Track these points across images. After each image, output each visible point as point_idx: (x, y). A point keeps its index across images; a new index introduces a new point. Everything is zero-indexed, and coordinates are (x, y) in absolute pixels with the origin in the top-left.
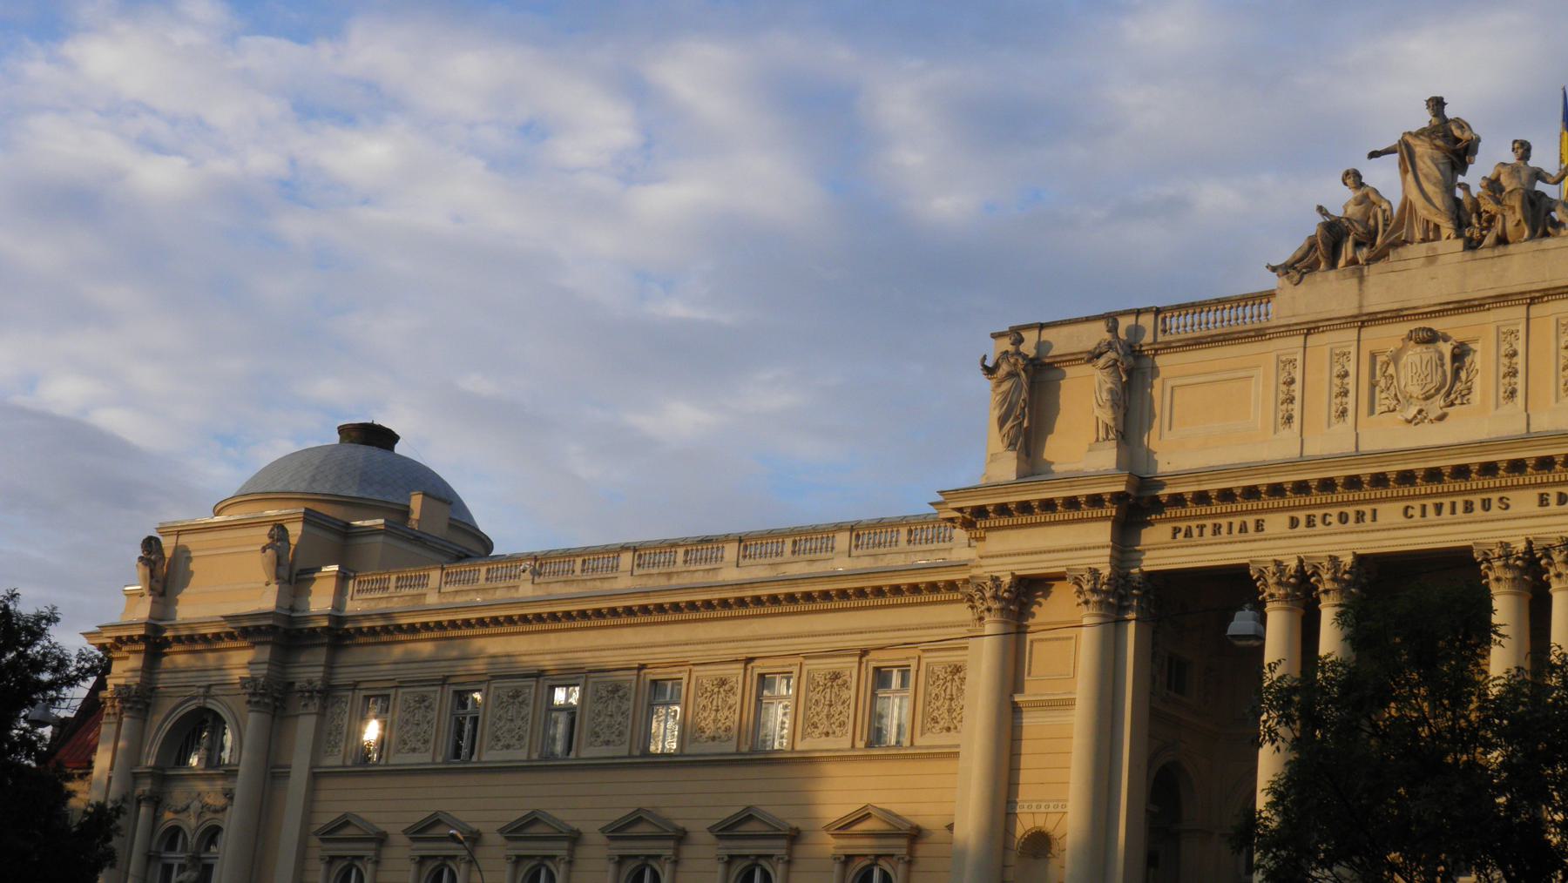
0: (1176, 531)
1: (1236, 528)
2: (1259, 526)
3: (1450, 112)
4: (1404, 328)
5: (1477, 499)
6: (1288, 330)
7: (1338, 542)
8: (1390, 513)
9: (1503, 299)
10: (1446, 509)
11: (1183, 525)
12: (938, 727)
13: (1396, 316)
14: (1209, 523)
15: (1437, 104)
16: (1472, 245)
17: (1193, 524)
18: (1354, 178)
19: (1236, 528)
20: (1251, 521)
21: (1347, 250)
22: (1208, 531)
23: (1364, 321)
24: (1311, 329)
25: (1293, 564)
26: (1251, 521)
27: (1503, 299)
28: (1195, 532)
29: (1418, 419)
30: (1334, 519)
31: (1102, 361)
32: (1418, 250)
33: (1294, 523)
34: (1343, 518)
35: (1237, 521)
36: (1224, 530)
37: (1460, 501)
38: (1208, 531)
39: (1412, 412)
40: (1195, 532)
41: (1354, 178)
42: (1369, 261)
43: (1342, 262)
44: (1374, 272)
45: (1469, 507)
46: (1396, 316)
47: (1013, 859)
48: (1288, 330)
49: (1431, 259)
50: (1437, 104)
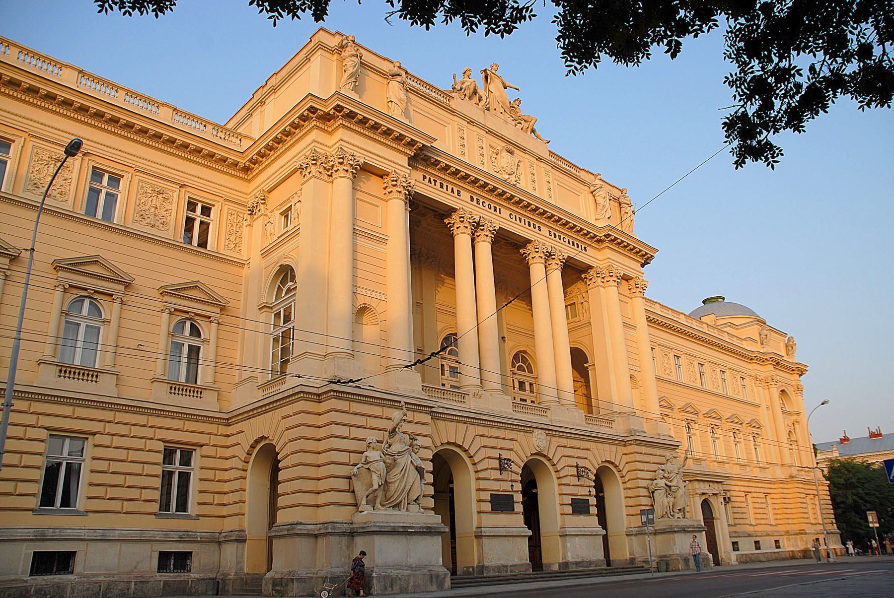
12: (144, 222)
23: (489, 132)
27: (531, 154)
28: (433, 182)
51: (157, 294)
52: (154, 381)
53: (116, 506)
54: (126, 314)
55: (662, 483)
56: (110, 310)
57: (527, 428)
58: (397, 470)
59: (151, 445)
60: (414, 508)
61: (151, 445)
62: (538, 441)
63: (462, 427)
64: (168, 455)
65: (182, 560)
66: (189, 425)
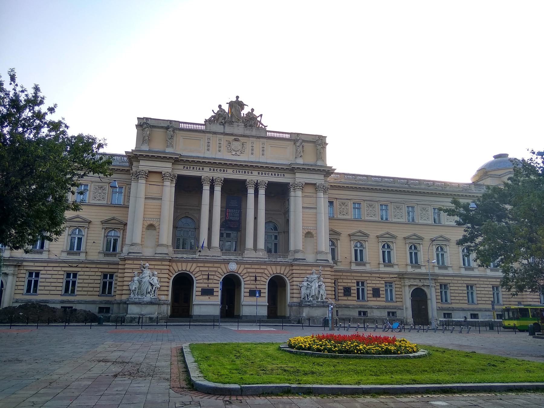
0: (184, 167)
1: (198, 169)
2: (203, 169)
3: (239, 100)
4: (234, 138)
5: (247, 171)
6: (209, 132)
7: (220, 175)
8: (230, 171)
9: (253, 137)
10: (241, 172)
11: (186, 166)
13: (232, 135)
14: (192, 167)
15: (237, 97)
16: (246, 126)
17: (188, 166)
18: (220, 106)
19: (198, 169)
20: (201, 168)
21: (221, 120)
22: (192, 168)
24: (215, 133)
25: (211, 178)
26: (201, 168)
27: (253, 137)
28: (189, 168)
29: (236, 154)
30: (219, 170)
31: (170, 129)
32: (235, 124)
33: (210, 170)
34: (220, 170)
35: (198, 167)
36: (195, 169)
37: (243, 171)
38: (192, 168)
39: (234, 153)
40: (189, 168)
41: (220, 106)
42: (225, 123)
43: (220, 121)
44: (226, 125)
45: (245, 173)
46: (232, 135)
47: (144, 230)
48: (209, 132)
49: (238, 126)
50: (237, 97)
51: (100, 223)
52: (99, 253)
53: (85, 293)
54: (89, 232)
55: (305, 284)
56: (84, 232)
57: (227, 262)
58: (142, 283)
59: (97, 274)
60: (148, 295)
61: (97, 274)
62: (233, 267)
63: (190, 265)
64: (105, 276)
65: (108, 310)
66: (111, 266)
